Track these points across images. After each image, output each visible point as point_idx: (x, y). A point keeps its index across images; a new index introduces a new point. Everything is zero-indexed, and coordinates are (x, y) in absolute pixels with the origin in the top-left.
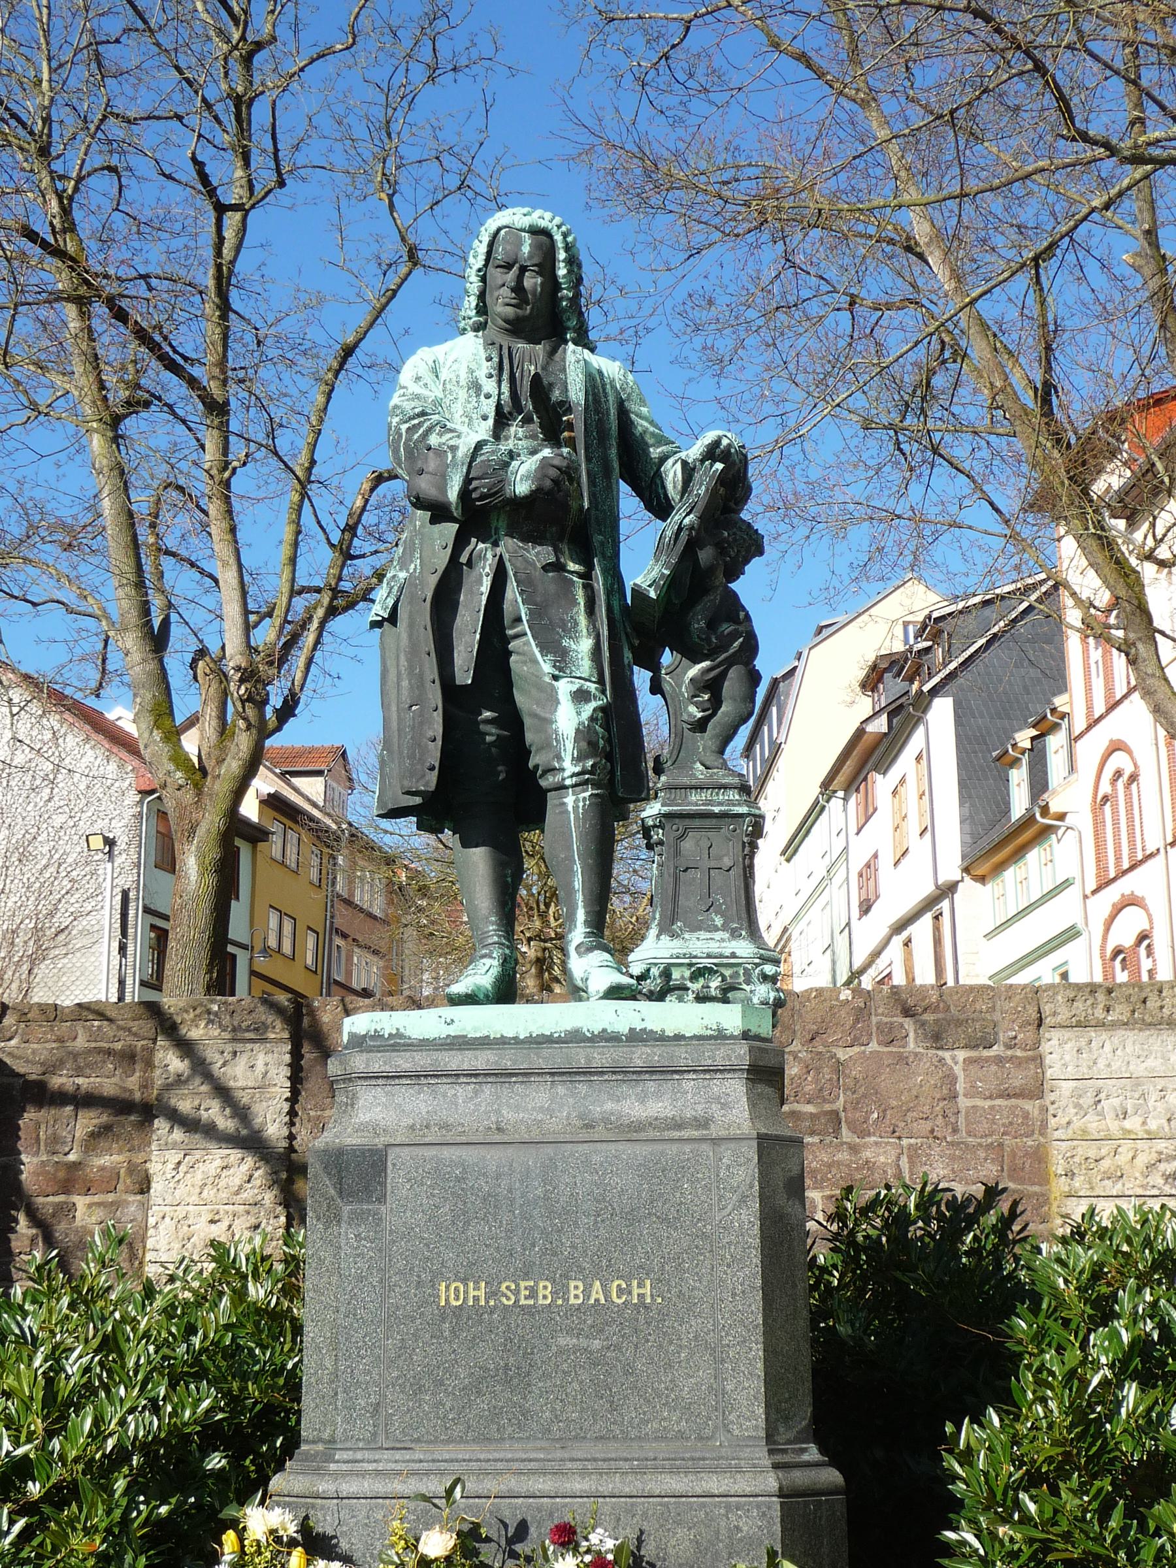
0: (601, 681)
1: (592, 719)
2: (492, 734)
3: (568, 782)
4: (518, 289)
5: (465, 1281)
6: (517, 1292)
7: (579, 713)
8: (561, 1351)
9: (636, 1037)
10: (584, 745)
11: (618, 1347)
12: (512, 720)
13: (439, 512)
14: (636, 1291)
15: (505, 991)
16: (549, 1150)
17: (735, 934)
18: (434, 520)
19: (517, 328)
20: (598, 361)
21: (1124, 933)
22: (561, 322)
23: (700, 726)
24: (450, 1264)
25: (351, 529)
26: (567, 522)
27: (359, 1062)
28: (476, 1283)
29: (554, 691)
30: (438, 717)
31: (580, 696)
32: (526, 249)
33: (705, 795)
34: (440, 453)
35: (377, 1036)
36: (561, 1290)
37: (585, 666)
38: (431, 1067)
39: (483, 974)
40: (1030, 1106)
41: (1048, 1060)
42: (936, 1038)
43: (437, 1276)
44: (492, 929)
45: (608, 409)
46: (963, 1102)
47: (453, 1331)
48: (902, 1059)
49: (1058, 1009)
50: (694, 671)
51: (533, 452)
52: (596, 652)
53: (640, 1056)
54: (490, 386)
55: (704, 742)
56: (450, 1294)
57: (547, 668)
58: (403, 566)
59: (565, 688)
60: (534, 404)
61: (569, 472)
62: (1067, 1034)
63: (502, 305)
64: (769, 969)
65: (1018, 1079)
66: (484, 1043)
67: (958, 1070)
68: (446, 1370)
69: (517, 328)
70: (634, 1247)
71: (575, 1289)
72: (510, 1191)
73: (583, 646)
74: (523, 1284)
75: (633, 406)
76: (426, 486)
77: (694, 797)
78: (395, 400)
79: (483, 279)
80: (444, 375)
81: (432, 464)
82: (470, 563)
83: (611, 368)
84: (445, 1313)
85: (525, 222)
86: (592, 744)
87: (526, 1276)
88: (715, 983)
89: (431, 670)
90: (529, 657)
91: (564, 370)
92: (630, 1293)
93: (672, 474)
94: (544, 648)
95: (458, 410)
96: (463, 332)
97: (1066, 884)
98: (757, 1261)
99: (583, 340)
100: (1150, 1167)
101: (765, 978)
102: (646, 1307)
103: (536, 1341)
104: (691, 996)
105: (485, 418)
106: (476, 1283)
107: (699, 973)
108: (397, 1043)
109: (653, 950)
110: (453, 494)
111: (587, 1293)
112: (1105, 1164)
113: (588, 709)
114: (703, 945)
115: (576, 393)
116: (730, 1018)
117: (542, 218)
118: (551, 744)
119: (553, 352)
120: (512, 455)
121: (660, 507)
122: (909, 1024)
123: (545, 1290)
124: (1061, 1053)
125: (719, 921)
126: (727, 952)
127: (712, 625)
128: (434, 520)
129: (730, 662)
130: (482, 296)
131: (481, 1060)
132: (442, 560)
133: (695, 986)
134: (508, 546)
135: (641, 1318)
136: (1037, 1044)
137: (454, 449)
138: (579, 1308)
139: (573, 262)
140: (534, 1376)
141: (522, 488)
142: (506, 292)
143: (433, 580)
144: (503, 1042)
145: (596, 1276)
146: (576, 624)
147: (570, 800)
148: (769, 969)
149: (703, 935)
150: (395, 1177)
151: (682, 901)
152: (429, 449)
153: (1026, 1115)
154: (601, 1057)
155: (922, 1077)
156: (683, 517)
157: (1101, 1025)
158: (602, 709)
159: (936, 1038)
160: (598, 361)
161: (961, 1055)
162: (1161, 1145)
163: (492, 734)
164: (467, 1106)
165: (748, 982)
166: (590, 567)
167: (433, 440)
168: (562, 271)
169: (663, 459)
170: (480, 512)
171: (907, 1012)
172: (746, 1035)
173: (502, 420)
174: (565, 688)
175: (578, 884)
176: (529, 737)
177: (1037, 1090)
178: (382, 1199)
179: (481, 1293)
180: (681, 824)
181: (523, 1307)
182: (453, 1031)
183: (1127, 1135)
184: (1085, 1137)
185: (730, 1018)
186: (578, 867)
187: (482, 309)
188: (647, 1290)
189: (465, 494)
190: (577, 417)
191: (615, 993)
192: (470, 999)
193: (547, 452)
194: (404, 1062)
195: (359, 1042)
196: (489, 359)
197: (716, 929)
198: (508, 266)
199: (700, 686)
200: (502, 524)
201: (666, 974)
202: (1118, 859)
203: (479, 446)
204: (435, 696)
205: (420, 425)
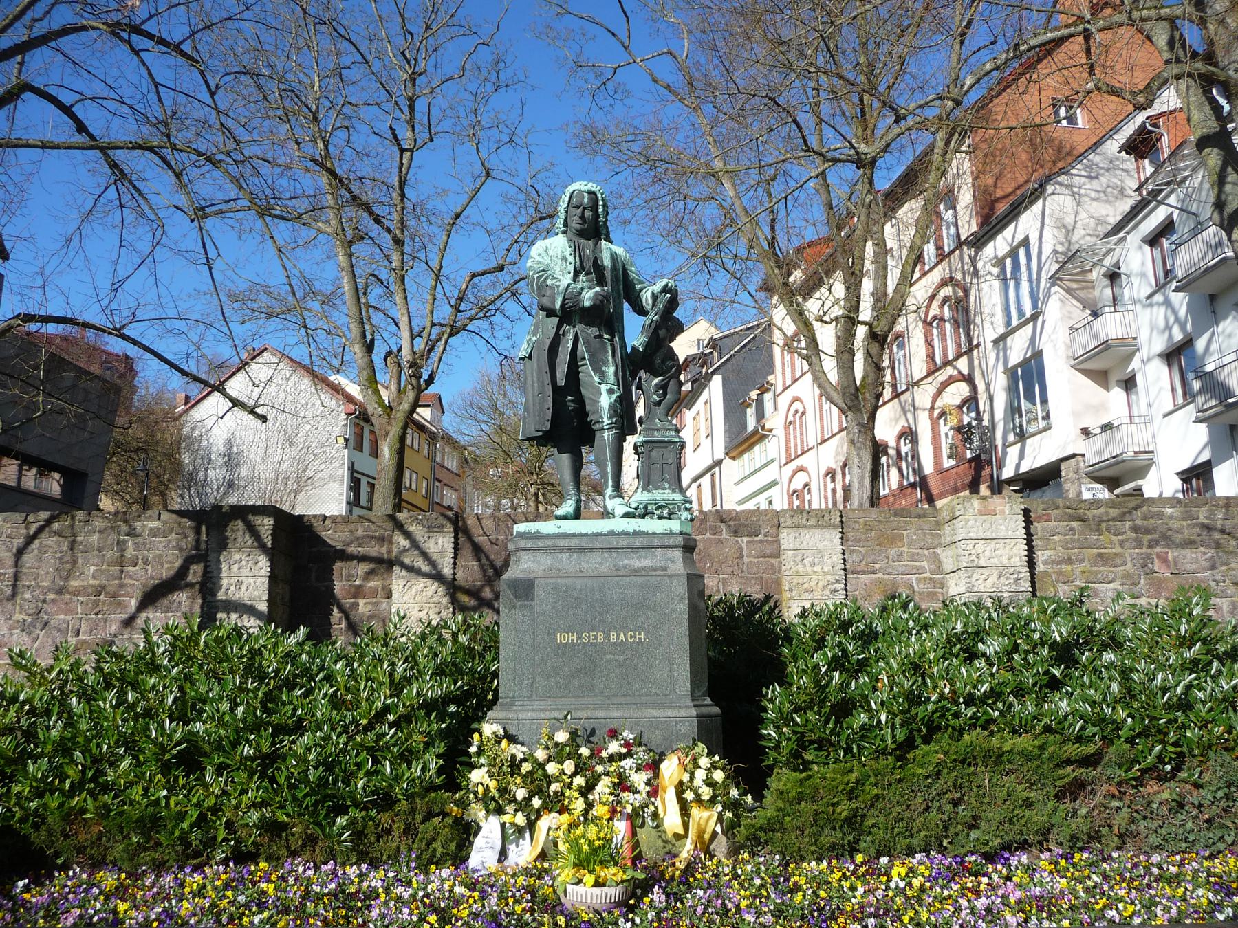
2: (571, 406)
4: (582, 217)
8: (607, 661)
9: (637, 534)
12: (580, 401)
13: (550, 313)
15: (577, 515)
16: (602, 580)
17: (674, 491)
18: (548, 316)
19: (581, 234)
20: (614, 248)
21: (798, 483)
23: (658, 404)
25: (460, 299)
26: (604, 318)
27: (521, 543)
29: (599, 390)
30: (550, 399)
32: (586, 200)
33: (661, 433)
34: (552, 288)
35: (529, 533)
36: (607, 636)
37: (612, 379)
38: (552, 545)
39: (568, 507)
40: (774, 561)
41: (782, 542)
42: (736, 533)
43: (556, 631)
44: (571, 488)
46: (746, 560)
48: (720, 541)
49: (787, 520)
50: (656, 381)
51: (591, 288)
52: (616, 372)
53: (638, 542)
54: (571, 259)
55: (660, 411)
56: (561, 638)
57: (596, 379)
58: (534, 334)
59: (604, 388)
60: (591, 268)
61: (606, 297)
62: (790, 531)
63: (575, 223)
64: (688, 506)
65: (769, 550)
66: (574, 536)
67: (744, 546)
69: (581, 234)
71: (613, 636)
73: (611, 370)
75: (628, 267)
76: (546, 302)
78: (529, 263)
80: (551, 253)
81: (548, 293)
82: (563, 334)
83: (620, 251)
85: (586, 188)
86: (615, 411)
88: (666, 511)
89: (547, 379)
90: (587, 373)
93: (646, 296)
95: (557, 269)
96: (557, 234)
97: (773, 461)
98: (687, 624)
99: (608, 239)
100: (825, 587)
101: (686, 509)
108: (537, 536)
109: (642, 497)
110: (558, 306)
112: (806, 586)
114: (661, 495)
115: (607, 262)
116: (674, 526)
117: (592, 187)
118: (598, 411)
120: (582, 289)
121: (641, 311)
122: (723, 526)
123: (601, 636)
124: (788, 539)
127: (663, 362)
128: (548, 316)
129: (671, 377)
130: (566, 219)
131: (573, 543)
132: (552, 333)
133: (658, 512)
134: (580, 327)
136: (777, 535)
137: (558, 286)
139: (605, 206)
141: (587, 304)
142: (577, 218)
143: (548, 342)
144: (581, 535)
147: (606, 435)
148: (688, 506)
150: (539, 591)
153: (773, 565)
154: (623, 542)
155: (729, 549)
156: (653, 317)
157: (805, 527)
159: (736, 533)
160: (614, 248)
161: (745, 539)
162: (829, 578)
163: (571, 406)
164: (568, 563)
166: (613, 337)
167: (549, 282)
168: (600, 210)
169: (641, 290)
170: (569, 313)
171: (723, 521)
172: (681, 533)
173: (576, 274)
174: (604, 388)
175: (609, 470)
176: (588, 408)
177: (777, 554)
178: (533, 600)
180: (651, 445)
182: (560, 531)
183: (815, 573)
184: (797, 574)
185: (674, 526)
187: (566, 225)
189: (563, 305)
190: (608, 273)
191: (627, 515)
192: (565, 517)
193: (598, 289)
194: (540, 544)
195: (521, 535)
198: (578, 207)
199: (658, 387)
200: (577, 318)
201: (646, 507)
202: (796, 450)
203: (569, 285)
204: (549, 390)
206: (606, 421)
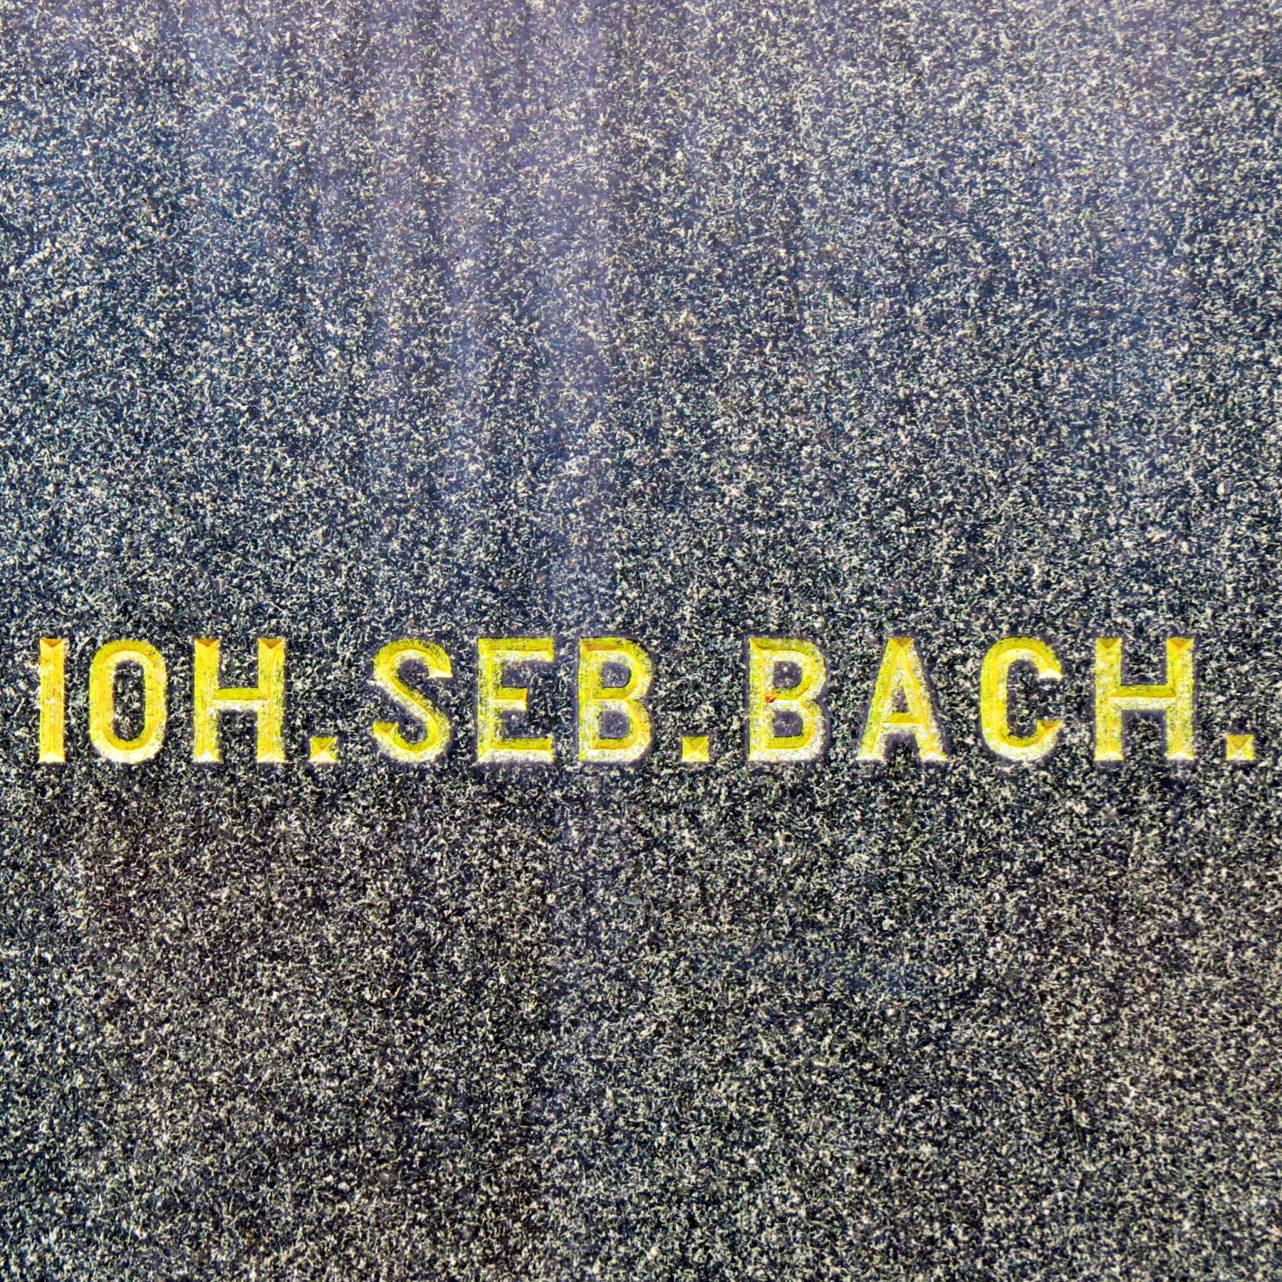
5: (174, 635)
6: (458, 701)
11: (1019, 999)
14: (1113, 700)
24: (93, 541)
28: (239, 646)
36: (701, 692)
47: (111, 903)
68: (74, 1109)
70: (1107, 466)
72: (427, 155)
74: (492, 656)
84: (60, 801)
87: (516, 610)
92: (1083, 707)
102: (1169, 784)
103: (567, 962)
106: (239, 646)
111: (845, 702)
123: (614, 693)
135: (1145, 845)
138: (800, 788)
140: (559, 1139)
145: (897, 619)
179: (265, 705)
181: (495, 782)
188: (1175, 696)
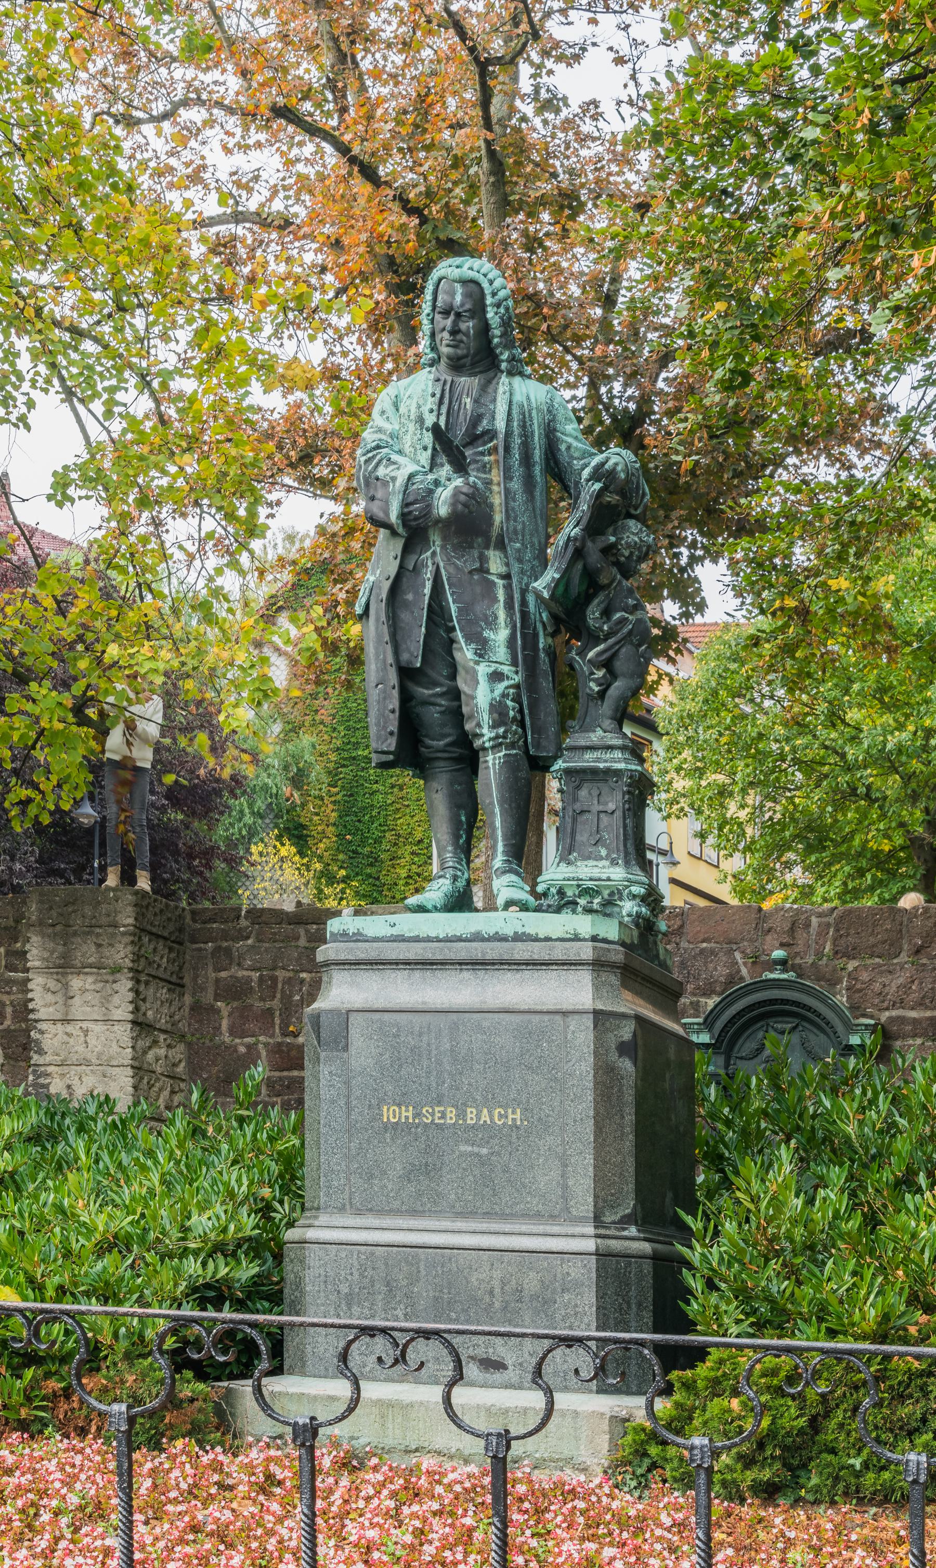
0: (514, 663)
1: (504, 695)
3: (487, 745)
4: (454, 332)
7: (492, 691)
10: (496, 716)
17: (614, 863)
22: (497, 356)
29: (475, 673)
31: (497, 677)
33: (597, 754)
37: (501, 653)
45: (533, 433)
59: (483, 670)
73: (500, 636)
76: (376, 509)
77: (588, 755)
79: (432, 321)
91: (494, 400)
94: (469, 639)
104: (579, 909)
105: (425, 448)
107: (586, 892)
110: (393, 517)
113: (500, 687)
119: (489, 382)
125: (604, 852)
126: (604, 876)
133: (582, 902)
137: (394, 479)
146: (496, 618)
149: (591, 863)
151: (578, 838)
152: (377, 479)
158: (517, 686)
165: (621, 899)
175: (498, 823)
186: (497, 810)
189: (403, 516)
196: (433, 395)
197: (601, 858)
205: (374, 457)
206: (487, 733)
